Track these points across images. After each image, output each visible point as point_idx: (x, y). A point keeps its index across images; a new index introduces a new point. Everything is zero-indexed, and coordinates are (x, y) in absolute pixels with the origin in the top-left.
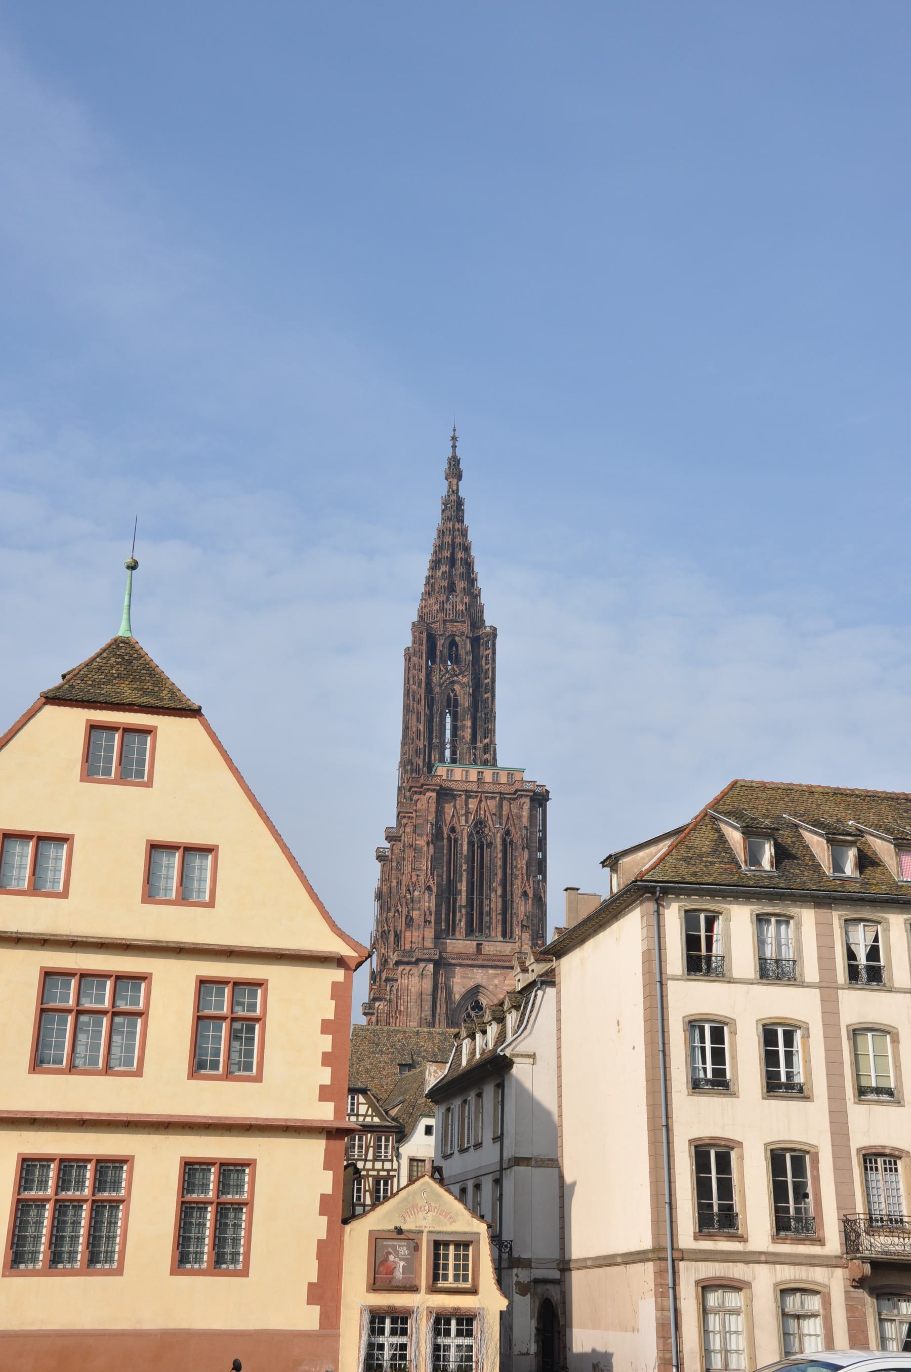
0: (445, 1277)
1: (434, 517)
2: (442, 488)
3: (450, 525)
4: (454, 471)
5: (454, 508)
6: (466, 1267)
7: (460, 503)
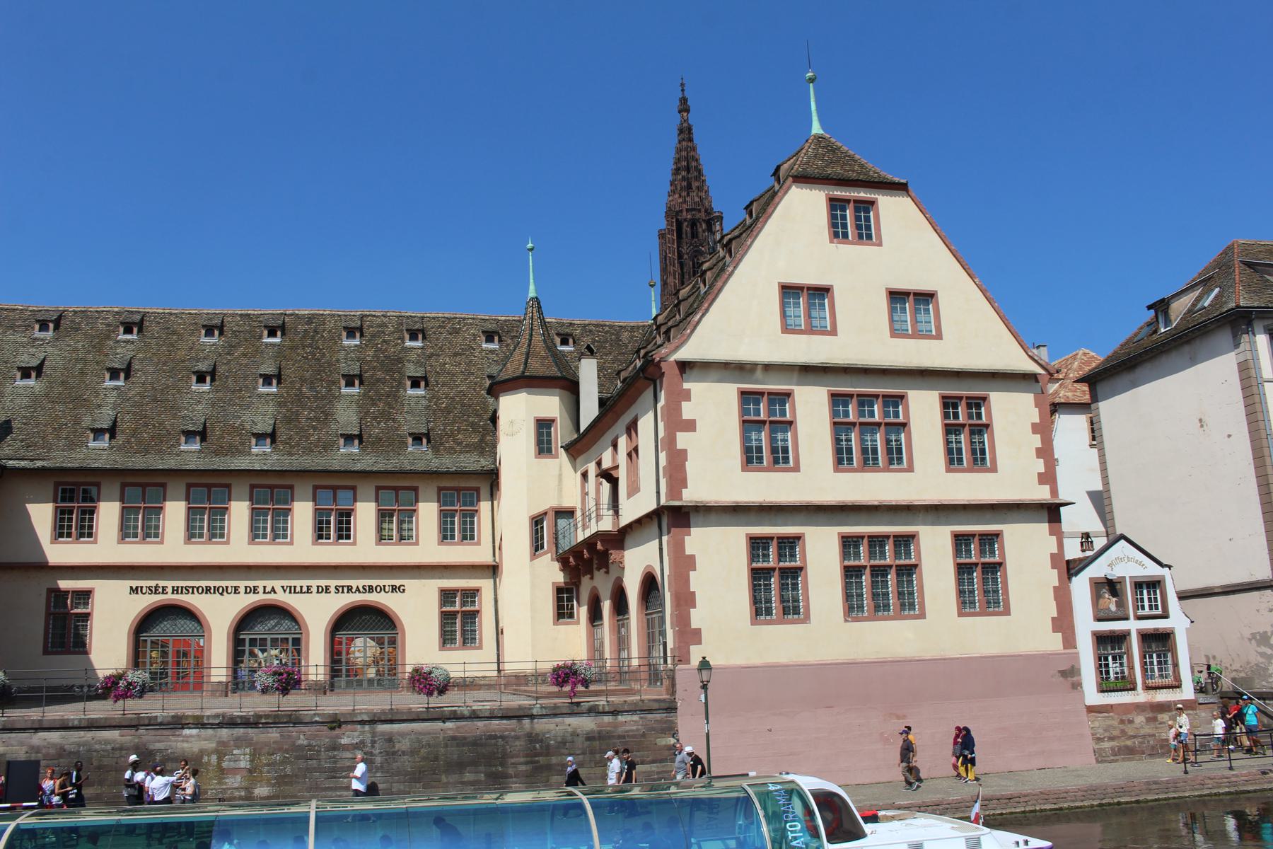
0: (1143, 607)
1: (671, 140)
2: (677, 119)
3: (684, 143)
4: (684, 107)
5: (686, 132)
6: (1156, 600)
7: (690, 129)
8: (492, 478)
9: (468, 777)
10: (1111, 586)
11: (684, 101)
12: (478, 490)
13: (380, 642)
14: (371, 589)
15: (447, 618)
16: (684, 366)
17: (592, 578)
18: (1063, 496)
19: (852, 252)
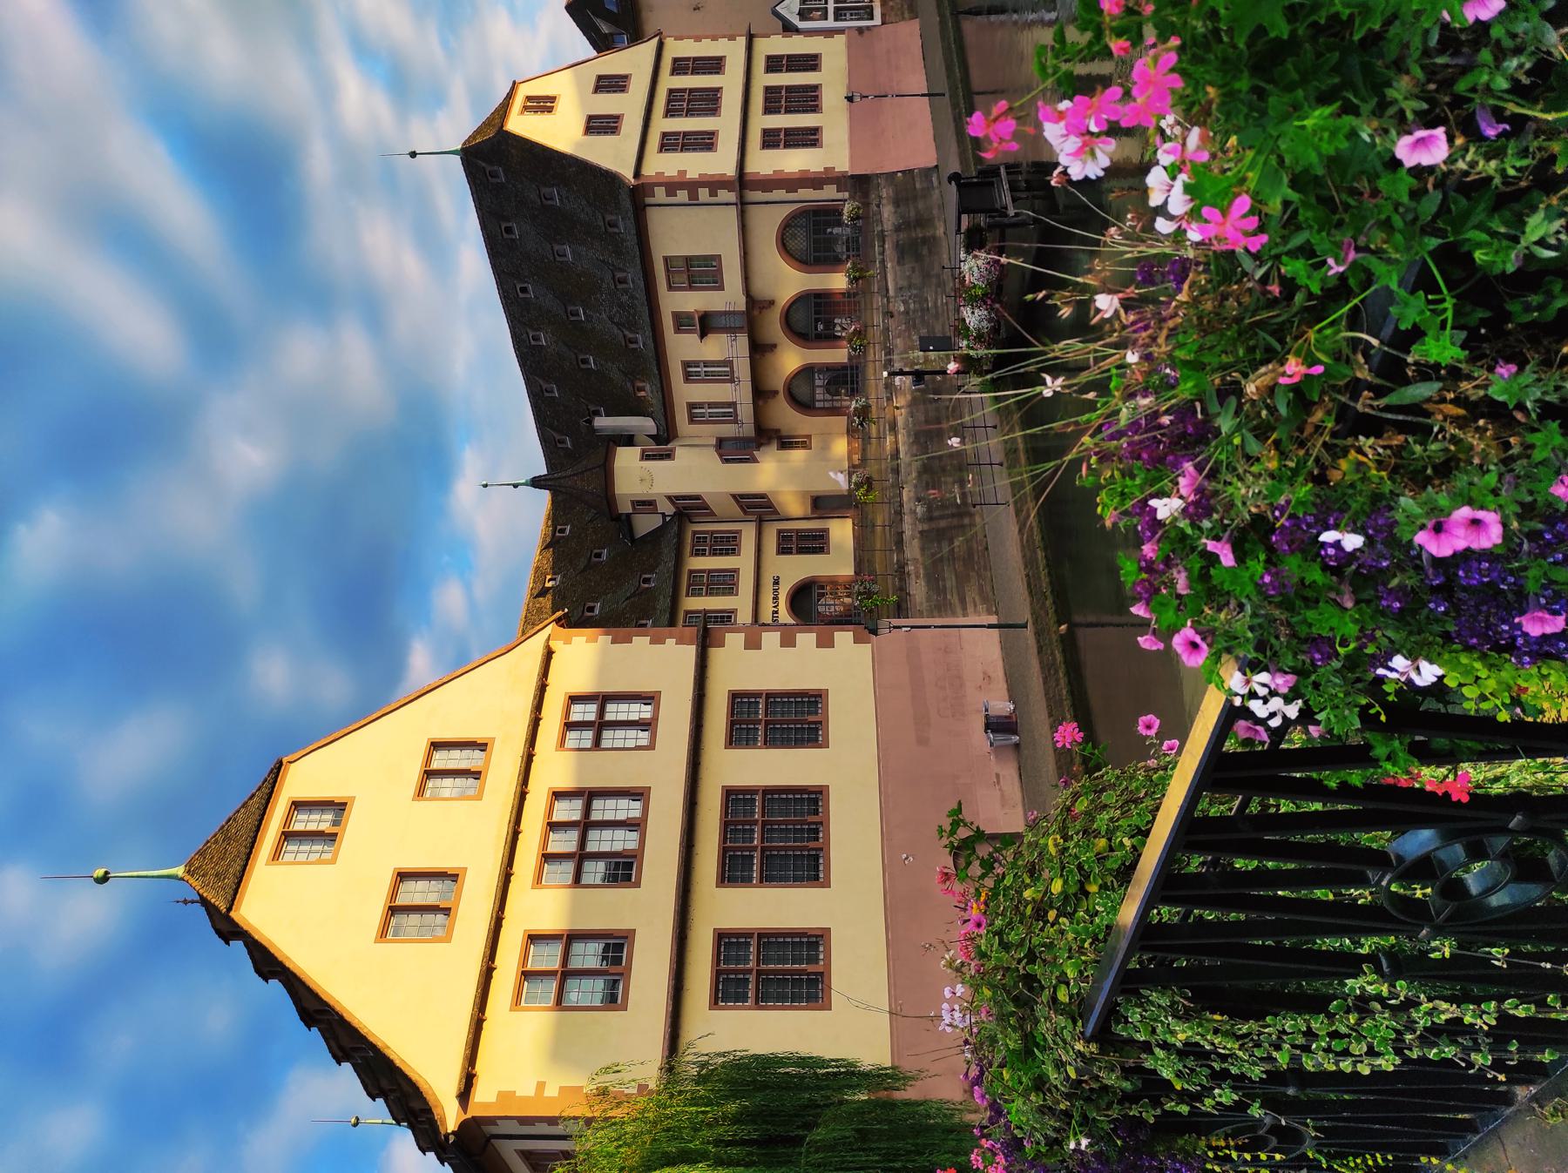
8: (688, 508)
9: (925, 252)
10: (803, 15)
12: (695, 533)
13: (823, 595)
14: (776, 598)
15: (801, 551)
16: (637, 174)
17: (776, 392)
18: (745, 31)
19: (560, 106)
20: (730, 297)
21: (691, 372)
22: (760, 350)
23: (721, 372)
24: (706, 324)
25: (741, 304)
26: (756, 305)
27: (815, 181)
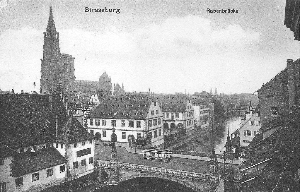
5: (51, 13)
11: (51, 7)
20: (175, 118)
21: (168, 114)
22: (170, 121)
23: (168, 117)
24: (172, 116)
25: (174, 119)
26: (174, 121)
27: (185, 127)
